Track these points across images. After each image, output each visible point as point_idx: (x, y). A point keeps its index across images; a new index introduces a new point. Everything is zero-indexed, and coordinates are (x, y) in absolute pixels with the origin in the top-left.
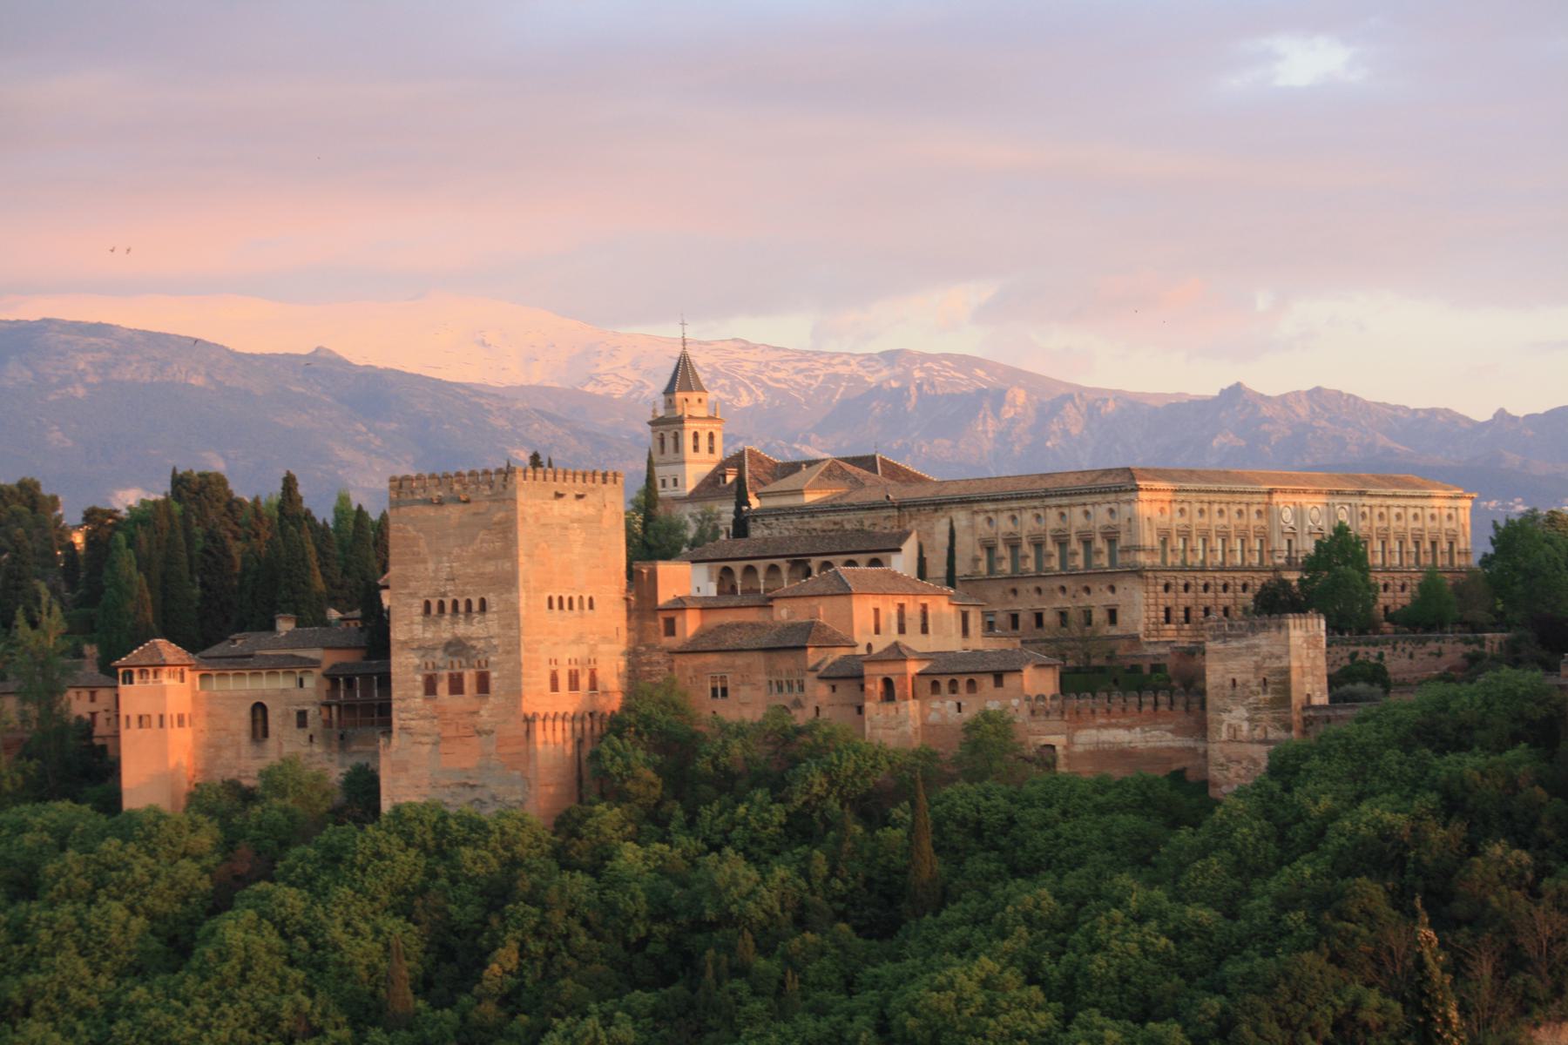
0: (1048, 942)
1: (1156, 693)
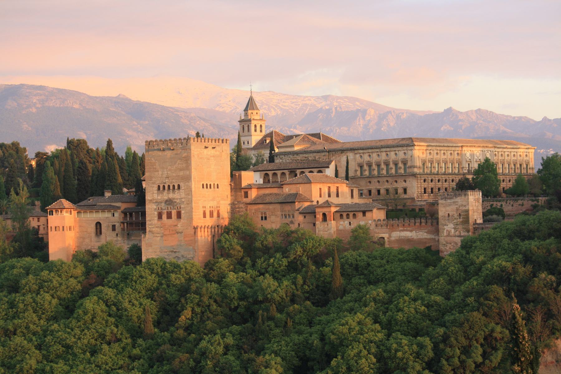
0: (382, 308)
1: (421, 219)
